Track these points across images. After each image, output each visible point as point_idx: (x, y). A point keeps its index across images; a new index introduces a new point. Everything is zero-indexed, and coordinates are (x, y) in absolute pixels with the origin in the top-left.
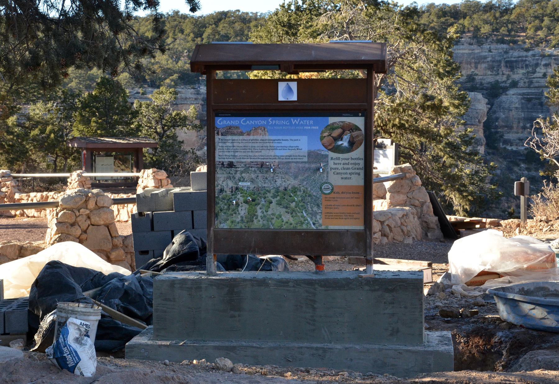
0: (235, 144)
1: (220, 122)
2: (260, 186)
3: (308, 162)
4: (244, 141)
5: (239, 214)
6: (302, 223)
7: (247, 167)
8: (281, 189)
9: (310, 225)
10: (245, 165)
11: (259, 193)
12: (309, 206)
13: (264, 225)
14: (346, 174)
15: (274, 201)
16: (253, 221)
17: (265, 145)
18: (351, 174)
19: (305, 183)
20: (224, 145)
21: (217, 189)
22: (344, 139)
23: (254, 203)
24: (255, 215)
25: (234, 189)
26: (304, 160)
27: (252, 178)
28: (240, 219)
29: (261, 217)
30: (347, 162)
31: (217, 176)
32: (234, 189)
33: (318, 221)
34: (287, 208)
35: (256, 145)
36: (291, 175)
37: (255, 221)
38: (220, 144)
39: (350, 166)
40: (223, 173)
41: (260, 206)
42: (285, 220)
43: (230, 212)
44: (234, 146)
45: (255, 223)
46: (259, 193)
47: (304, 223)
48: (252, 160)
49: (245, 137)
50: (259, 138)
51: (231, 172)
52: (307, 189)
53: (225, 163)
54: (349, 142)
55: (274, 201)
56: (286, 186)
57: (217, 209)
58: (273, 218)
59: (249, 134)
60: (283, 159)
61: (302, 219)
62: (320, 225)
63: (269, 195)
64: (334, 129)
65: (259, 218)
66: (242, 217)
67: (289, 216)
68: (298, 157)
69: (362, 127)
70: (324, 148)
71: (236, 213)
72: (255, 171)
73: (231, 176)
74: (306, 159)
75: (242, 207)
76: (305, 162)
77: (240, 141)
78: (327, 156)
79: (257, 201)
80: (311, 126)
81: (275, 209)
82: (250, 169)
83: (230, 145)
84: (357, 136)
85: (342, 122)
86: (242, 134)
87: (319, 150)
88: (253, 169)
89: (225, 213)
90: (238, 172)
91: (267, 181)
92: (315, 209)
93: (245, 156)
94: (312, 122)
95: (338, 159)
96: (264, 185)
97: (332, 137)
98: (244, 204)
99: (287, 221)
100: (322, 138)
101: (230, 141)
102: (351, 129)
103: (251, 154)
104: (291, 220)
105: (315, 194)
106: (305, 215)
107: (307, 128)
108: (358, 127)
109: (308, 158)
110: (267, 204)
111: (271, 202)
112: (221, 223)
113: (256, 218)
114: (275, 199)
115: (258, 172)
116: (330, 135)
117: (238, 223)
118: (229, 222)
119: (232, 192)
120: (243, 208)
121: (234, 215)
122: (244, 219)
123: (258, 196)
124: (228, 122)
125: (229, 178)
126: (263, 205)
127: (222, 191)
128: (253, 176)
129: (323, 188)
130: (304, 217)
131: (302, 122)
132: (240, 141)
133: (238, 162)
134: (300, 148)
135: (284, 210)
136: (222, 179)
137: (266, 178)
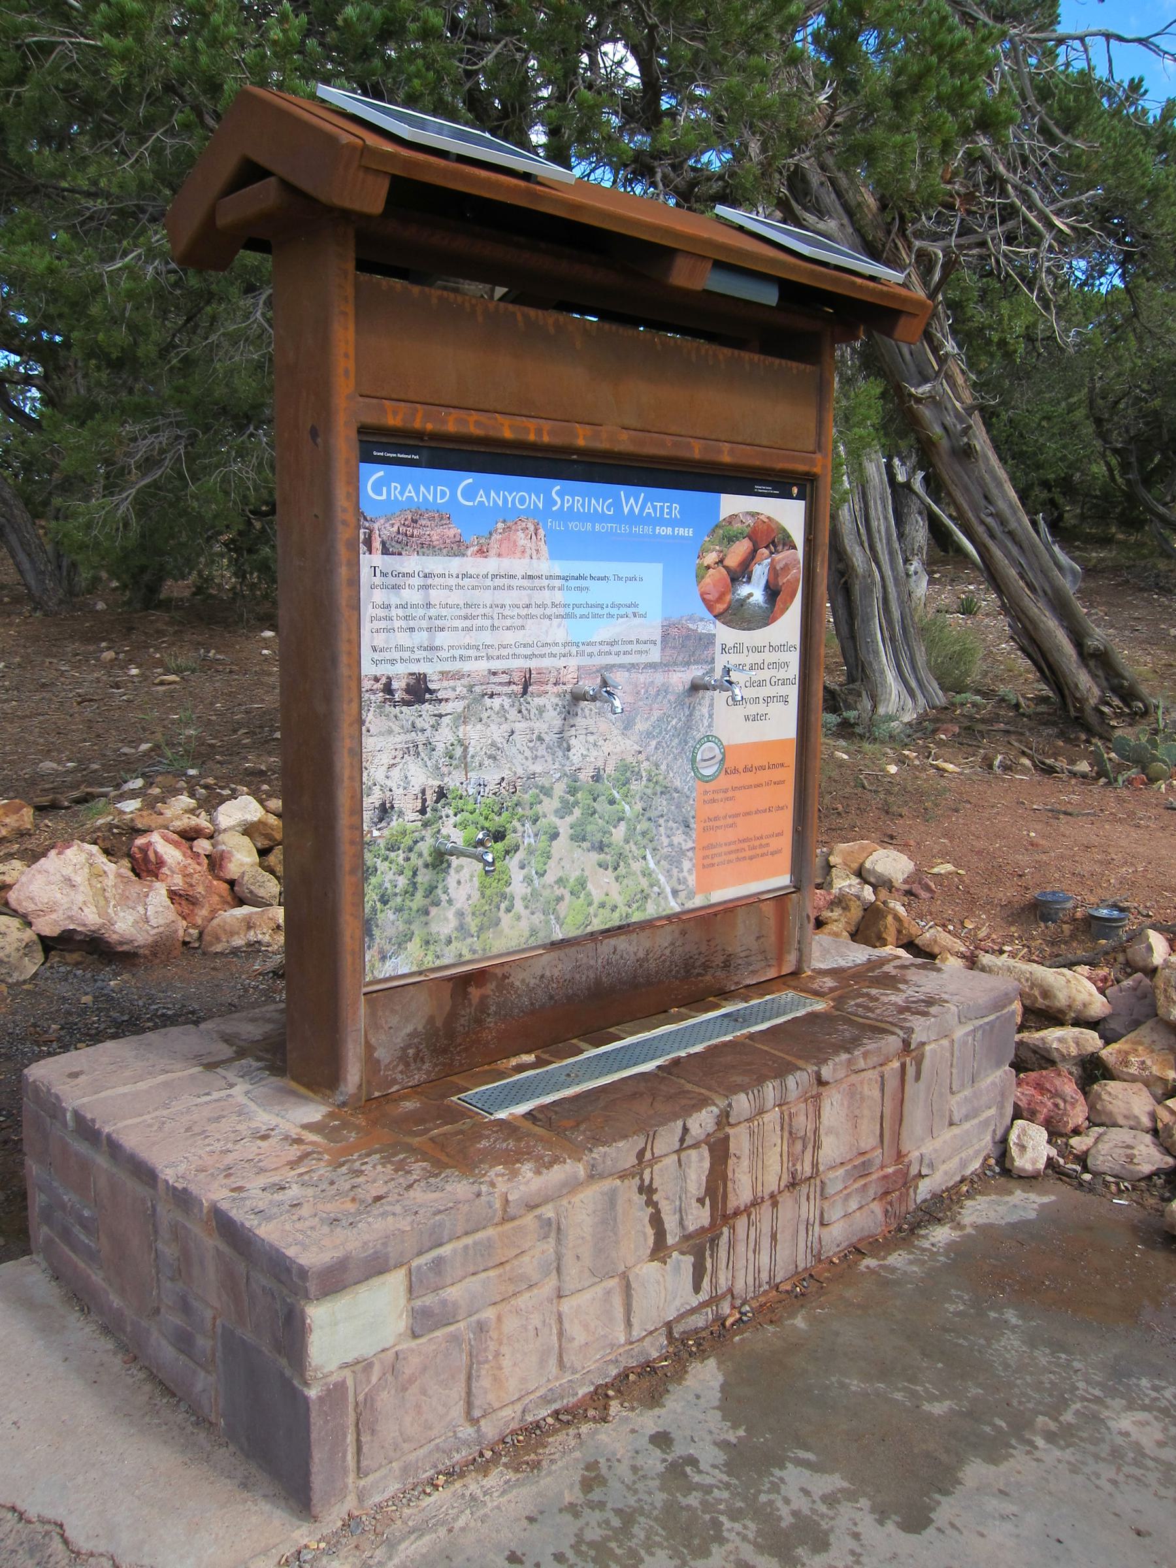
0: (435, 596)
1: (377, 489)
2: (520, 772)
4: (467, 581)
5: (450, 902)
7: (478, 696)
8: (585, 776)
10: (470, 688)
13: (533, 932)
14: (756, 700)
16: (498, 922)
17: (538, 597)
18: (767, 700)
19: (653, 743)
22: (754, 577)
23: (499, 846)
24: (504, 896)
25: (431, 797)
27: (493, 744)
28: (453, 922)
30: (756, 658)
31: (369, 743)
34: (601, 848)
35: (508, 598)
37: (506, 919)
38: (379, 596)
39: (765, 674)
40: (390, 732)
41: (520, 855)
42: (597, 896)
43: (419, 900)
44: (429, 605)
45: (507, 931)
48: (496, 665)
49: (469, 563)
50: (518, 566)
51: (420, 723)
52: (657, 766)
53: (395, 685)
54: (767, 587)
56: (600, 764)
58: (560, 899)
59: (482, 552)
60: (591, 655)
63: (549, 806)
64: (731, 539)
65: (519, 906)
67: (608, 877)
68: (636, 647)
69: (798, 536)
70: (702, 610)
73: (421, 738)
74: (655, 655)
76: (652, 666)
77: (452, 582)
78: (710, 639)
79: (511, 838)
80: (673, 523)
81: (571, 860)
84: (786, 568)
85: (753, 514)
86: (457, 548)
87: (691, 618)
88: (497, 701)
89: (399, 910)
90: (446, 720)
92: (678, 838)
93: (468, 647)
95: (737, 648)
99: (603, 898)
101: (416, 581)
102: (773, 543)
103: (487, 637)
106: (652, 865)
108: (789, 536)
111: (555, 836)
112: (383, 958)
113: (508, 910)
114: (569, 819)
115: (513, 714)
116: (721, 561)
117: (449, 942)
118: (414, 947)
119: (423, 811)
120: (465, 874)
121: (434, 911)
122: (469, 919)
124: (410, 491)
125: (412, 750)
126: (531, 852)
127: (385, 811)
128: (497, 732)
129: (699, 757)
131: (649, 509)
132: (452, 582)
134: (640, 610)
135: (595, 856)
136: (386, 759)
137: (540, 739)
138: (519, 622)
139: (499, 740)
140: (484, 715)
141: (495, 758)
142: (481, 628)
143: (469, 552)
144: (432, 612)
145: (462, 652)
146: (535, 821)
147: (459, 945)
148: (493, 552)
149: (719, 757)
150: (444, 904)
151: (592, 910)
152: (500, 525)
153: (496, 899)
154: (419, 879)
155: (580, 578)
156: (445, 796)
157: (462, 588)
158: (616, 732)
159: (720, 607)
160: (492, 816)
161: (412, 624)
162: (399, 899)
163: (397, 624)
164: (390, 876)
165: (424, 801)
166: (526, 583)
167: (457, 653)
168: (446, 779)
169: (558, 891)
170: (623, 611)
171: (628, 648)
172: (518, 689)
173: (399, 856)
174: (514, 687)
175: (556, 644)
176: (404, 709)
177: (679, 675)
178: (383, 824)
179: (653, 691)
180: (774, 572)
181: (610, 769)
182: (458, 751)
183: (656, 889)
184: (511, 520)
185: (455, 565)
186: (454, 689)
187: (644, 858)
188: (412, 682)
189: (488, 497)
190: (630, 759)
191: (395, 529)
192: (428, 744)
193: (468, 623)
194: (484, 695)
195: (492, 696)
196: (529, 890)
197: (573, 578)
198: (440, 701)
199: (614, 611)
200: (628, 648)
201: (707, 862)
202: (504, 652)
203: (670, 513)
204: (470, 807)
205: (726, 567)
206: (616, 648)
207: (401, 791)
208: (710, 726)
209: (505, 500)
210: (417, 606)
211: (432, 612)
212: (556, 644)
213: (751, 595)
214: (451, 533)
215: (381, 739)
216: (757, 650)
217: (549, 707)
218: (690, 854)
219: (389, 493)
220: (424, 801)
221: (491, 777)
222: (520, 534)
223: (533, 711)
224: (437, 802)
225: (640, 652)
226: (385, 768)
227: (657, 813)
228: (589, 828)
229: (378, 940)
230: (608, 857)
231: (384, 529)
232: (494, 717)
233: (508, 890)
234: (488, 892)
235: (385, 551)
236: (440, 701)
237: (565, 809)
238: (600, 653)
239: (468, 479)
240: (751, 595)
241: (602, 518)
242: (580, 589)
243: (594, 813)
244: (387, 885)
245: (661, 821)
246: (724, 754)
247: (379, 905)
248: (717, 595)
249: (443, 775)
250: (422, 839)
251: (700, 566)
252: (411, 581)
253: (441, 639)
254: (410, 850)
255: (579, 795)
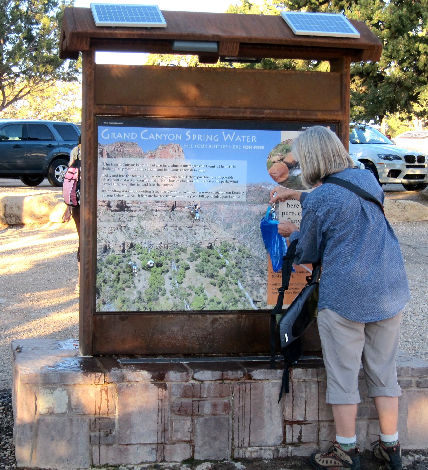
0: (130, 172)
1: (105, 135)
2: (170, 241)
3: (249, 203)
4: (145, 167)
5: (135, 287)
6: (236, 301)
7: (149, 211)
8: (204, 246)
9: (249, 303)
10: (146, 207)
11: (169, 253)
12: (247, 273)
15: (192, 265)
16: (157, 299)
19: (242, 236)
20: (112, 173)
21: (100, 246)
23: (159, 269)
24: (161, 289)
25: (127, 247)
26: (240, 200)
27: (157, 229)
28: (136, 296)
29: (171, 292)
32: (127, 247)
33: (261, 298)
34: (212, 276)
36: (219, 223)
37: (162, 299)
38: (105, 172)
40: (109, 221)
41: (169, 274)
42: (210, 296)
44: (127, 176)
45: (162, 303)
46: (169, 253)
47: (239, 301)
48: (157, 199)
49: (147, 161)
50: (169, 162)
51: (122, 219)
52: (244, 246)
53: (112, 204)
55: (192, 265)
56: (212, 241)
57: (99, 280)
58: (189, 295)
59: (152, 156)
60: (207, 197)
61: (237, 295)
62: (265, 304)
65: (168, 294)
66: (140, 293)
67: (216, 289)
68: (231, 195)
71: (129, 287)
72: (162, 217)
73: (123, 224)
74: (243, 198)
75: (140, 275)
76: (242, 203)
77: (139, 167)
79: (164, 267)
81: (194, 279)
82: (155, 213)
83: (122, 173)
86: (141, 155)
87: (264, 184)
88: (159, 213)
91: (181, 233)
92: (257, 278)
93: (145, 192)
94: (254, 138)
96: (176, 240)
97: (287, 164)
98: (143, 272)
99: (213, 298)
100: (269, 165)
101: (122, 167)
104: (219, 296)
105: (257, 254)
106: (241, 287)
107: (247, 147)
109: (247, 196)
110: (181, 270)
111: (187, 268)
112: (104, 303)
113: (163, 295)
114: (195, 263)
115: (167, 218)
116: (282, 160)
117: (134, 302)
118: (118, 302)
119: (123, 251)
120: (142, 278)
122: (143, 295)
123: (166, 257)
124: (120, 135)
127: (106, 249)
128: (159, 225)
130: (240, 292)
131: (238, 138)
132: (139, 167)
133: (133, 202)
135: (209, 280)
136: (107, 230)
137: (180, 229)
138: (170, 183)
139: (160, 228)
140: (153, 218)
141: (158, 235)
142: (152, 185)
143: (146, 156)
144: (129, 178)
145: (143, 194)
146: (177, 261)
147: (139, 305)
148: (157, 156)
150: (132, 287)
151: (206, 302)
152: (161, 147)
153: (157, 290)
154: (121, 276)
156: (133, 247)
157: (143, 170)
158: (221, 229)
159: (282, 179)
160: (155, 257)
161: (120, 182)
162: (112, 283)
163: (113, 182)
164: (108, 273)
165: (124, 248)
166: (173, 168)
167: (140, 194)
168: (134, 241)
169: (189, 291)
170: (224, 180)
171: (228, 195)
172: (170, 209)
173: (112, 267)
174: (168, 208)
175: (188, 192)
176: (116, 213)
177: (258, 208)
178: (105, 254)
179: (242, 214)
181: (218, 244)
182: (140, 231)
183: (243, 298)
184: (166, 144)
185: (140, 161)
186: (139, 207)
187: (236, 284)
188: (119, 203)
189: (155, 136)
191: (113, 148)
192: (126, 226)
193: (146, 183)
194: (152, 210)
195: (156, 211)
196: (174, 288)
197: (197, 166)
198: (132, 211)
199: (220, 180)
200: (228, 195)
202: (163, 194)
203: (251, 140)
204: (146, 252)
205: (285, 162)
207: (114, 243)
209: (163, 137)
210: (122, 176)
212: (188, 192)
214: (138, 149)
215: (105, 223)
217: (185, 216)
219: (110, 136)
220: (124, 248)
221: (156, 242)
222: (170, 149)
223: (177, 218)
224: (130, 248)
225: (235, 197)
226: (107, 234)
227: (244, 266)
228: (206, 268)
229: (102, 296)
230: (216, 281)
232: (157, 218)
233: (163, 287)
234: (153, 286)
235: (109, 156)
236: (132, 211)
237: (193, 259)
238: (212, 197)
241: (213, 142)
243: (209, 261)
244: (107, 277)
247: (103, 284)
248: (280, 174)
249: (133, 239)
250: (123, 261)
251: (269, 162)
252: (120, 167)
253: (132, 188)
254: (117, 265)
255: (201, 254)
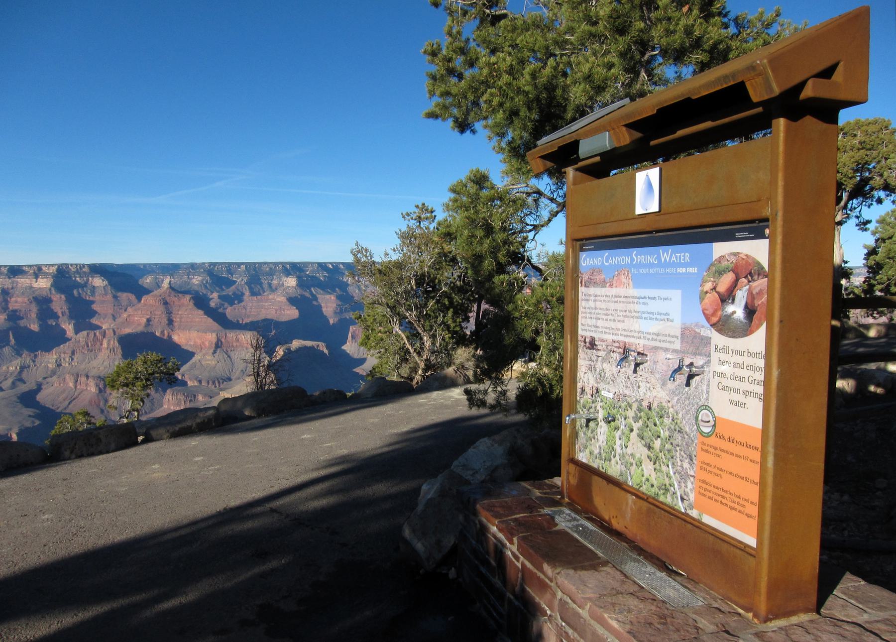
8: (645, 404)
14: (737, 391)
19: (676, 399)
44: (596, 308)
50: (621, 291)
59: (611, 286)
60: (649, 339)
64: (720, 273)
68: (668, 339)
80: (686, 265)
85: (735, 254)
86: (603, 284)
92: (686, 465)
95: (725, 350)
101: (593, 298)
103: (612, 325)
116: (714, 288)
134: (670, 317)
138: (622, 319)
142: (610, 320)
149: (712, 423)
155: (644, 298)
159: (714, 320)
166: (624, 300)
170: (662, 317)
171: (665, 338)
180: (751, 296)
184: (619, 269)
190: (664, 404)
199: (659, 317)
200: (665, 338)
201: (702, 491)
202: (618, 332)
205: (717, 292)
206: (659, 338)
208: (707, 399)
211: (597, 311)
213: (734, 312)
216: (740, 353)
218: (692, 479)
225: (670, 342)
231: (585, 277)
237: (637, 419)
239: (606, 253)
240: (734, 312)
241: (651, 265)
242: (644, 303)
245: (678, 448)
246: (715, 421)
251: (702, 291)
